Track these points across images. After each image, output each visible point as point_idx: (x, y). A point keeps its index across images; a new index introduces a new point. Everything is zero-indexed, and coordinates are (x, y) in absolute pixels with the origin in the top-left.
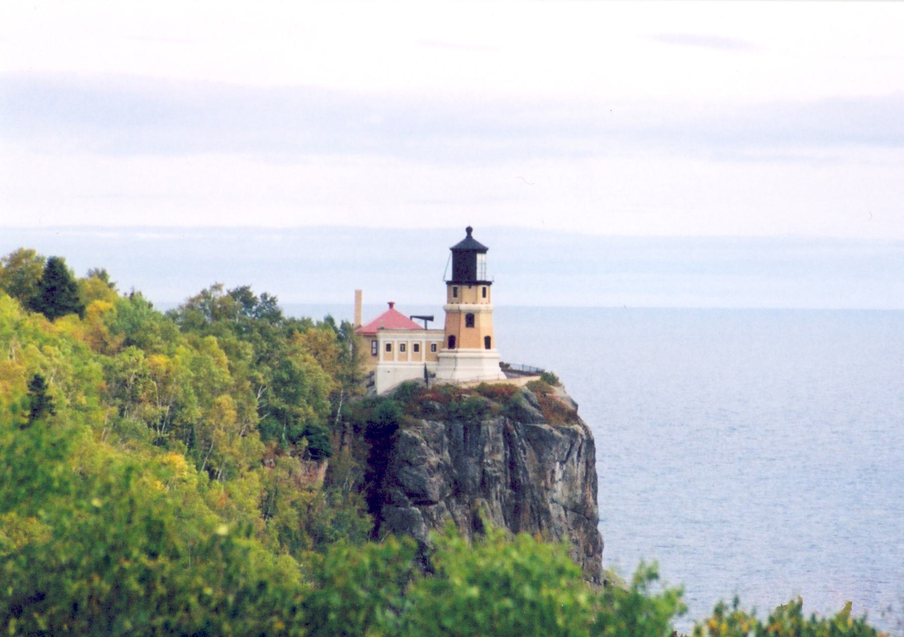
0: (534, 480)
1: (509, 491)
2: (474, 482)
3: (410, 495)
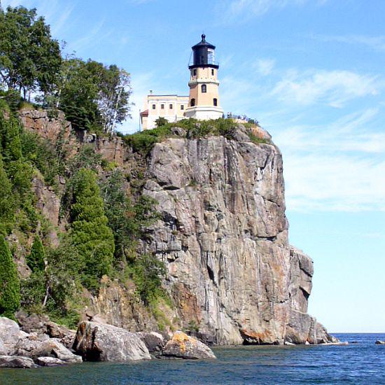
1: (227, 185)
2: (204, 177)
3: (161, 184)
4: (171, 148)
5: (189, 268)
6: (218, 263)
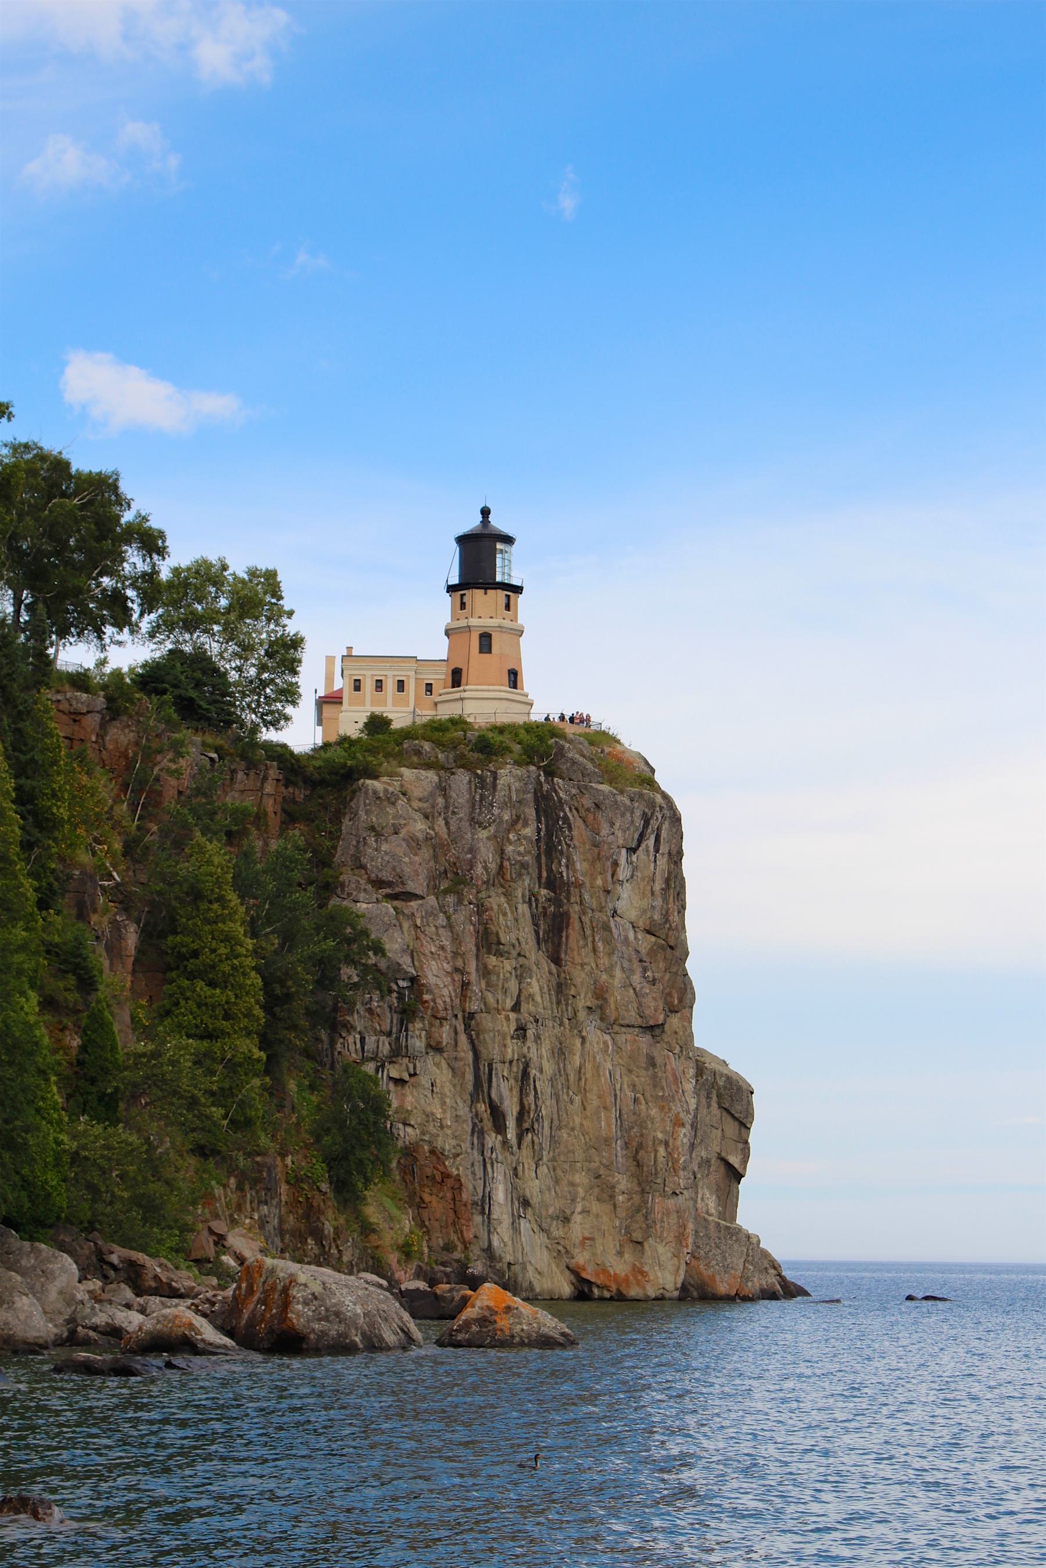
0: (585, 874)
1: (544, 892)
3: (378, 883)
4: (404, 794)
5: (443, 1103)
6: (516, 1092)
